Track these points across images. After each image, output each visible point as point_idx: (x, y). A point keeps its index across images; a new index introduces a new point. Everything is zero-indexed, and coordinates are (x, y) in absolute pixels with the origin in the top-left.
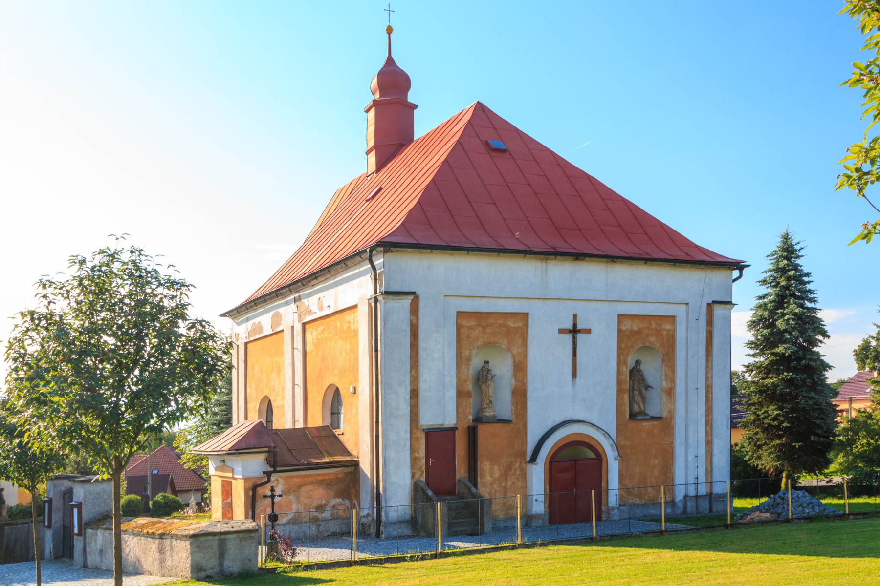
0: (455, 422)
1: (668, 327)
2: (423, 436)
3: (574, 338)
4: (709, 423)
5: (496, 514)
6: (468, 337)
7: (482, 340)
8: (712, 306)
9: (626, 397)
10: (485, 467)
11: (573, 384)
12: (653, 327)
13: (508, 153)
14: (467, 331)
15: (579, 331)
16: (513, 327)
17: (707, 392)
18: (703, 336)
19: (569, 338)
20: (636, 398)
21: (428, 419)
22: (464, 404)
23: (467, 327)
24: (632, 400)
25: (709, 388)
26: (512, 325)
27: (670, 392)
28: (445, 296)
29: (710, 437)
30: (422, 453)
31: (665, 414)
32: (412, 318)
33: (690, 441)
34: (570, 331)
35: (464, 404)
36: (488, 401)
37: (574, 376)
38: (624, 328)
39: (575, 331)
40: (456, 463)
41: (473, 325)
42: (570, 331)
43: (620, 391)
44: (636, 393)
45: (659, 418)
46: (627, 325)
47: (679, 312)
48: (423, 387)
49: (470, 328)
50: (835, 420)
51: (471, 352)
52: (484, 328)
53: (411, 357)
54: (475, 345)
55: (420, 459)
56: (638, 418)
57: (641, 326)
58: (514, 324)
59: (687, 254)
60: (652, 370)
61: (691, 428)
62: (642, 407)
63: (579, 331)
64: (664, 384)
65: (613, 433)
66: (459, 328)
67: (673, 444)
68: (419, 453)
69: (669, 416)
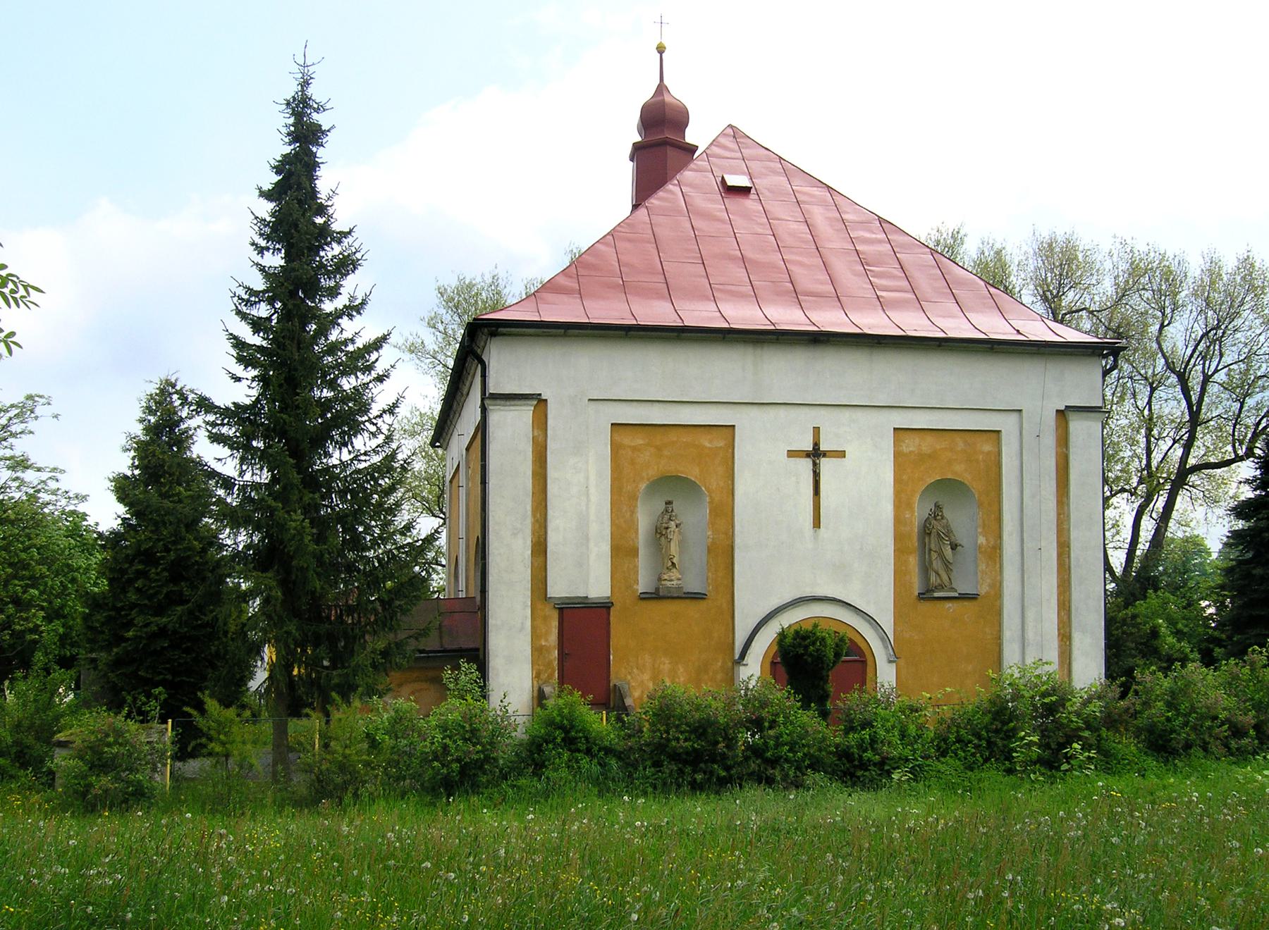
0: (609, 594)
1: (987, 447)
2: (555, 614)
3: (815, 464)
4: (1065, 606)
5: (357, 703)
6: (633, 462)
7: (656, 467)
8: (1066, 413)
9: (913, 562)
10: (662, 666)
11: (814, 538)
12: (959, 449)
13: (753, 196)
14: (630, 453)
15: (825, 454)
16: (709, 448)
17: (1060, 555)
18: (1050, 463)
19: (807, 464)
20: (934, 563)
21: (559, 588)
22: (626, 566)
23: (630, 447)
24: (926, 569)
25: (1064, 547)
26: (708, 445)
27: (995, 552)
28: (589, 400)
29: (1068, 630)
30: (553, 638)
31: (983, 589)
32: (536, 434)
33: (1030, 635)
34: (808, 455)
35: (626, 566)
36: (670, 564)
37: (817, 523)
38: (905, 449)
39: (816, 454)
40: (611, 657)
41: (641, 445)
42: (808, 455)
43: (900, 551)
44: (934, 555)
45: (971, 597)
46: (911, 445)
47: (1006, 423)
48: (553, 538)
49: (634, 449)
50: (337, 456)
51: (637, 487)
52: (659, 449)
53: (533, 493)
54: (644, 474)
55: (548, 649)
56: (936, 595)
57: (938, 447)
58: (711, 442)
59: (1018, 331)
60: (961, 521)
61: (1031, 615)
62: (945, 577)
63: (825, 454)
64: (982, 540)
65: (887, 622)
66: (616, 448)
67: (1000, 639)
68: (546, 640)
69: (993, 593)
